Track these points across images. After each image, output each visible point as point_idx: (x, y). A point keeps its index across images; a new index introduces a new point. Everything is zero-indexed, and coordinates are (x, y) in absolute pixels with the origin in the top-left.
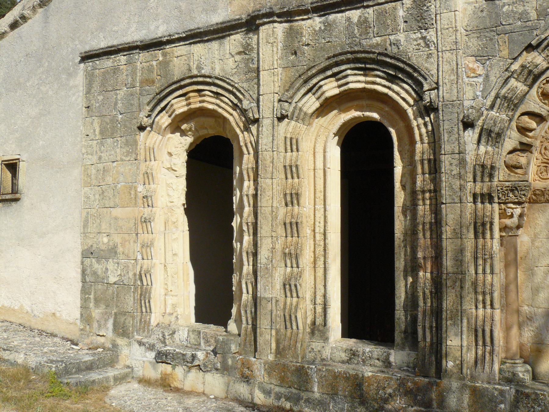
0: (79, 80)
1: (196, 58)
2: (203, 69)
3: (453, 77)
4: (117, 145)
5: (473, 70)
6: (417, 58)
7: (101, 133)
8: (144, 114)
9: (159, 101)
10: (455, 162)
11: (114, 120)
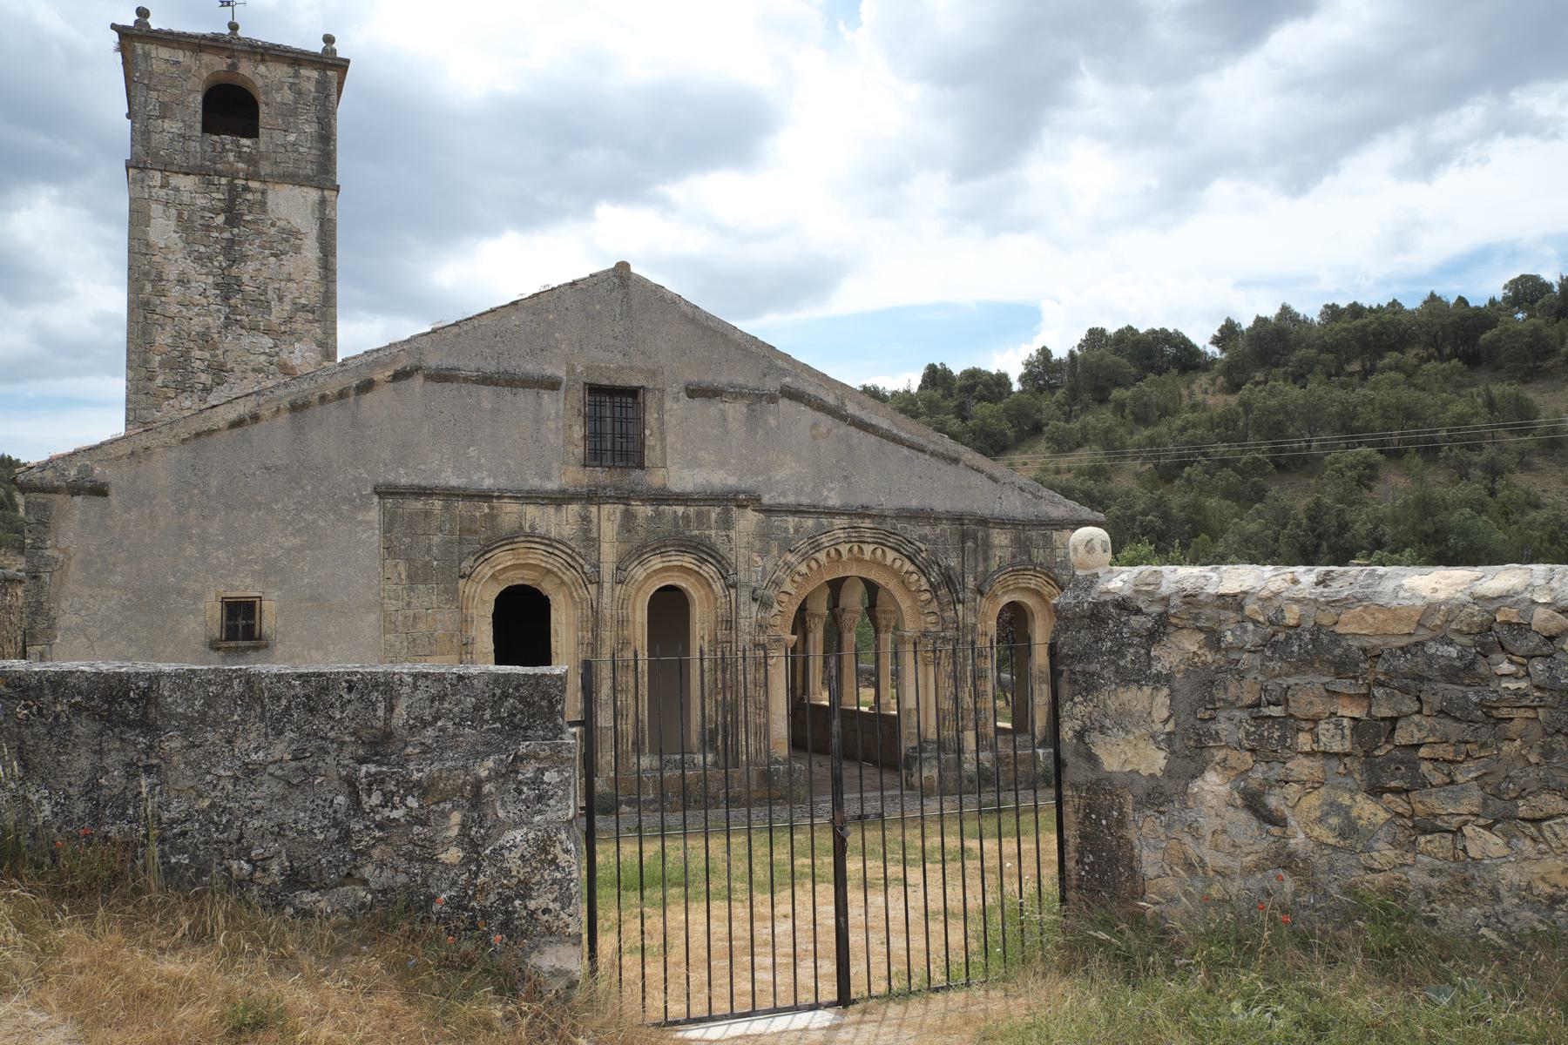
0: (374, 515)
6: (723, 549)
7: (409, 577)
9: (486, 550)
11: (427, 565)
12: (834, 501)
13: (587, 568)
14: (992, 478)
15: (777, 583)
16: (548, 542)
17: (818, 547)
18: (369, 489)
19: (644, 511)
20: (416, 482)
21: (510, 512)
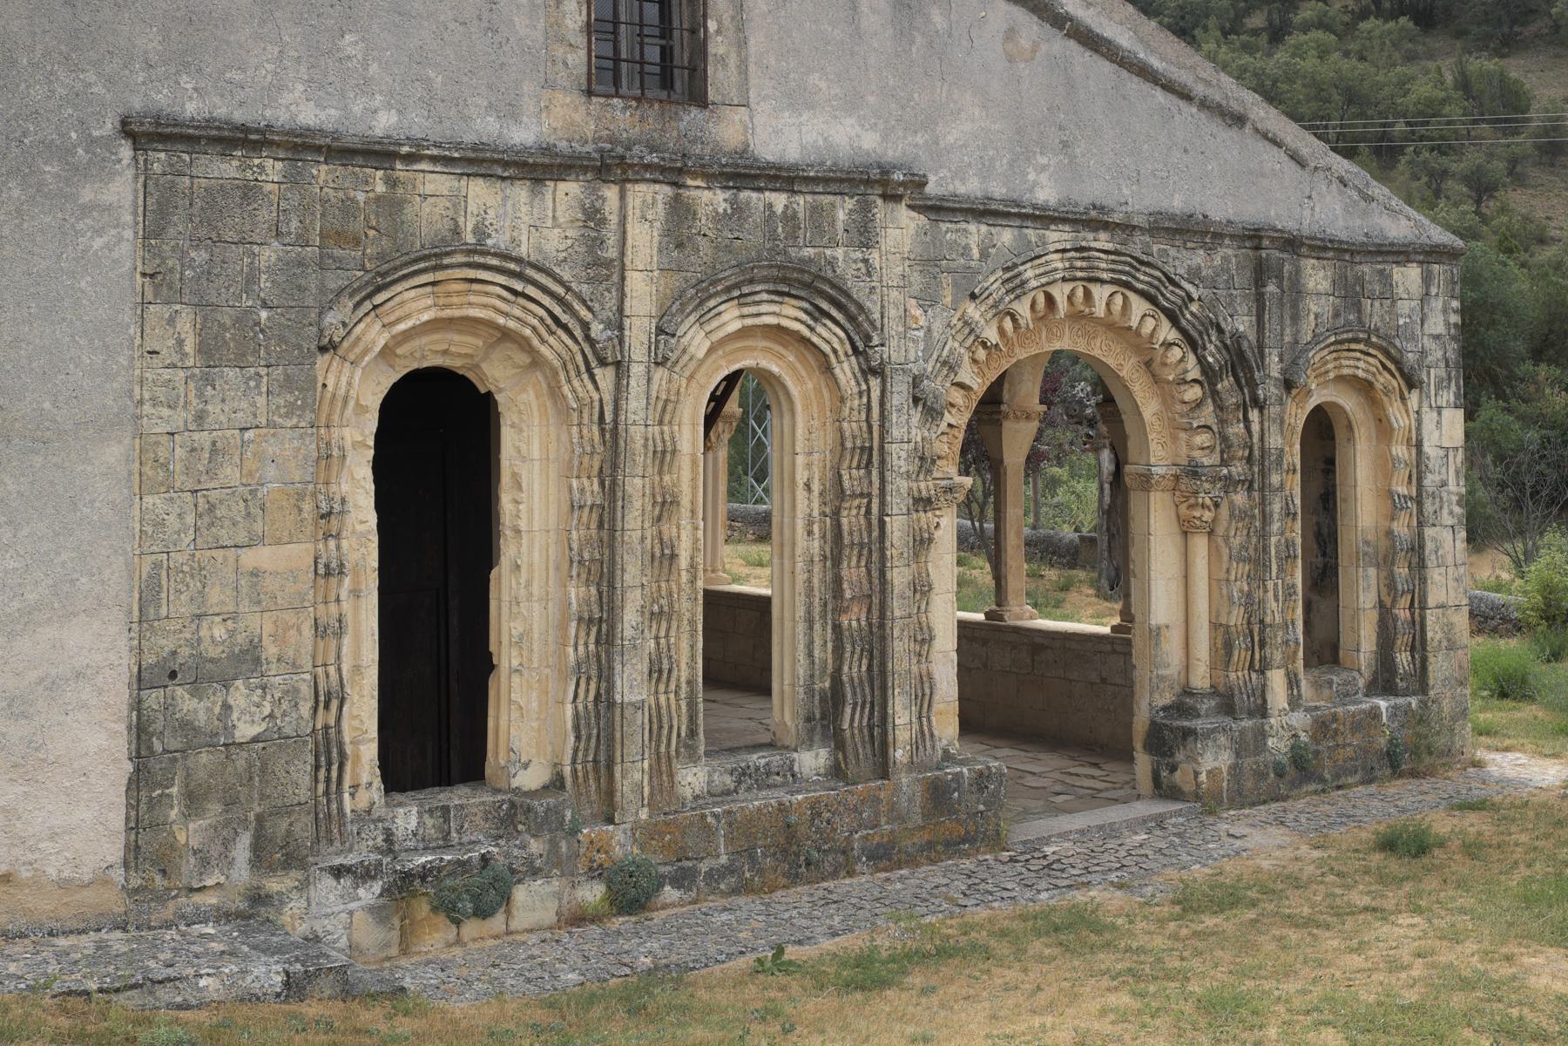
0: (120, 189)
1: (472, 207)
2: (489, 236)
3: (901, 329)
4: (258, 386)
5: (916, 319)
6: (858, 290)
7: (202, 349)
8: (340, 317)
10: (903, 455)
11: (244, 320)
12: (1046, 194)
13: (597, 329)
14: (1296, 158)
15: (950, 366)
16: (515, 267)
17: (1017, 287)
18: (109, 126)
19: (711, 200)
20: (221, 112)
21: (434, 197)
